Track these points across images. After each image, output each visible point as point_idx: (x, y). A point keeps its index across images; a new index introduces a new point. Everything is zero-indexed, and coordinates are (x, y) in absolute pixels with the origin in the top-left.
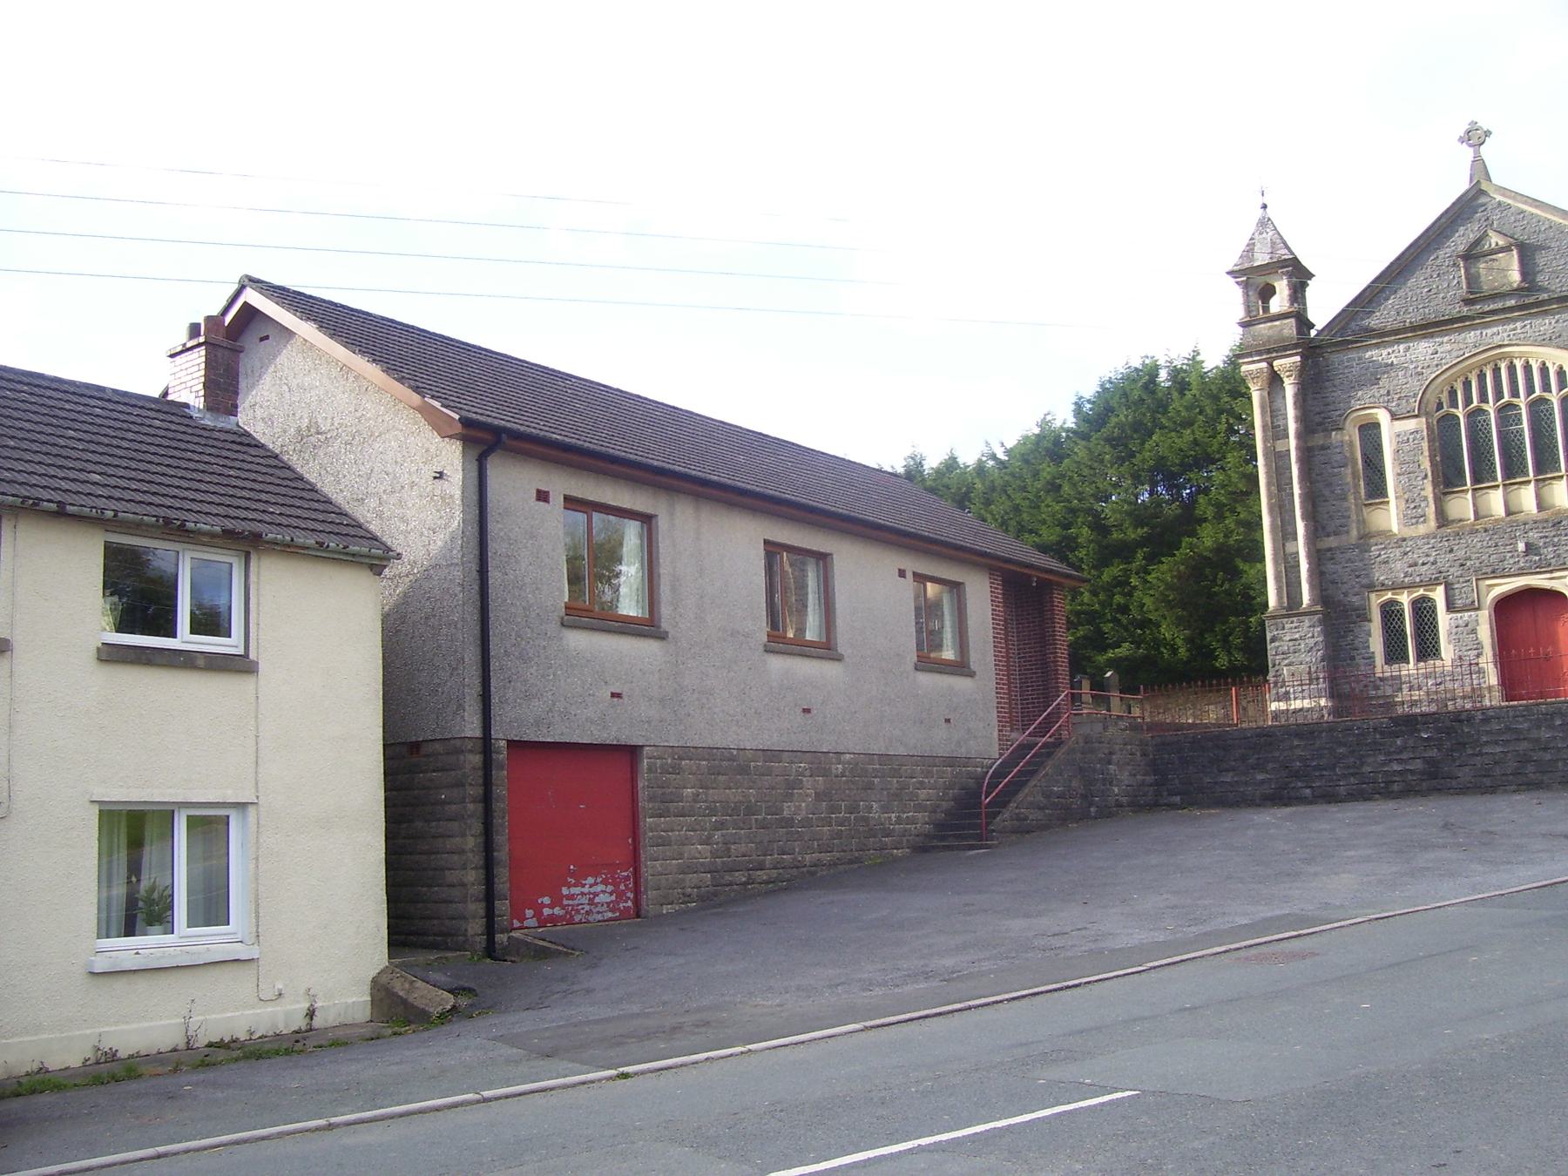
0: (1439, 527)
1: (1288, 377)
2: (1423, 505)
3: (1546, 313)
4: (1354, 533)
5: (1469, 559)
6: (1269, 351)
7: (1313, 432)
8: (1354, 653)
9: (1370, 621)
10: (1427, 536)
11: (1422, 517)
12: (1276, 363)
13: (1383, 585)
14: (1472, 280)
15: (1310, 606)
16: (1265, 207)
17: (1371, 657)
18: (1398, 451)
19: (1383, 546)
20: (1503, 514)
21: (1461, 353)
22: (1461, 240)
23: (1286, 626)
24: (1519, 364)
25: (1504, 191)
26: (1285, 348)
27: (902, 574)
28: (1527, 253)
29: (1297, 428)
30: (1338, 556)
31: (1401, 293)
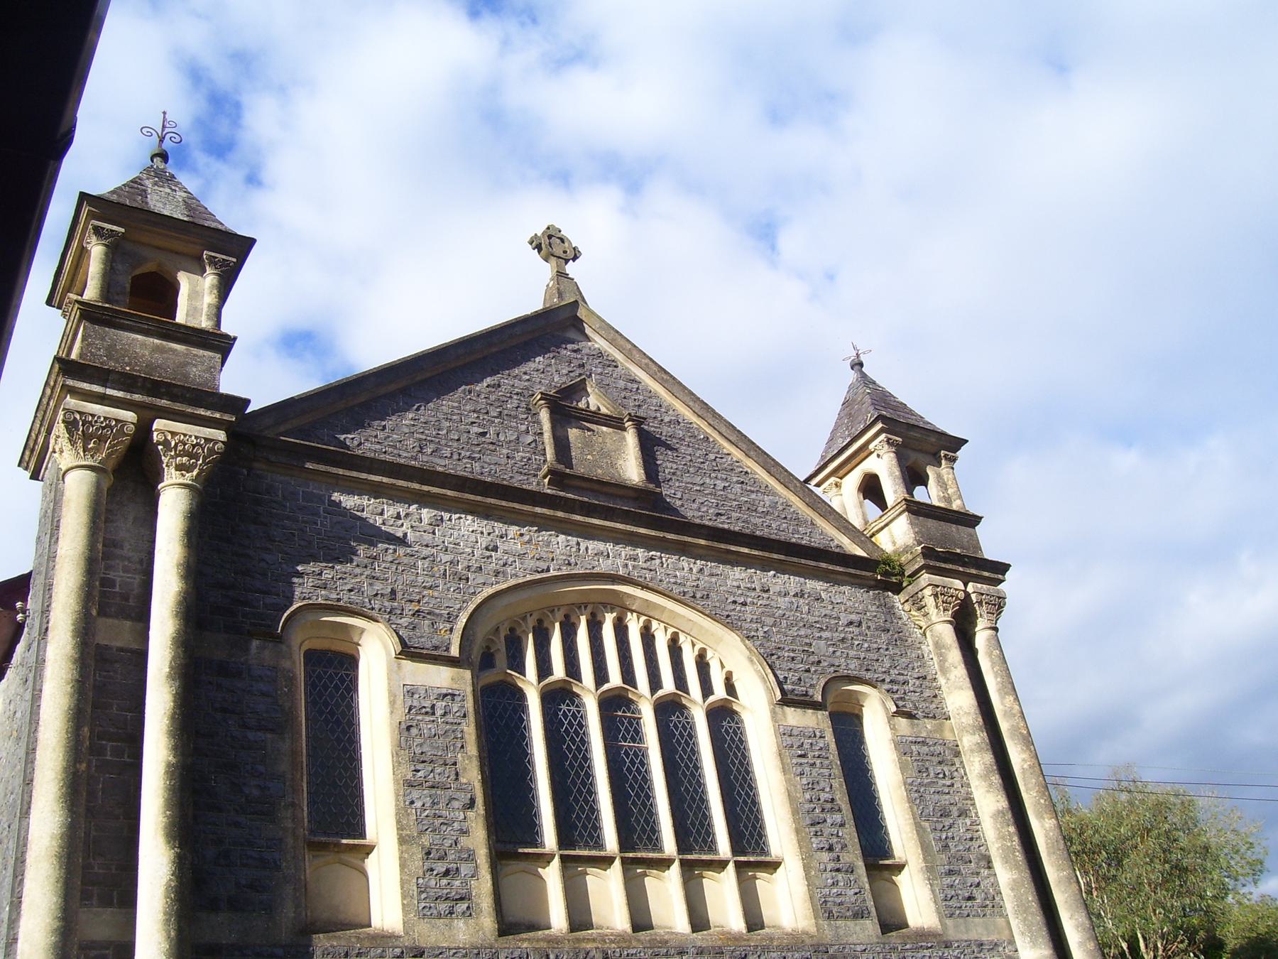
1: (180, 468)
2: (465, 869)
11: (462, 899)
12: (159, 424)
18: (409, 728)
21: (543, 565)
25: (615, 336)
28: (649, 445)
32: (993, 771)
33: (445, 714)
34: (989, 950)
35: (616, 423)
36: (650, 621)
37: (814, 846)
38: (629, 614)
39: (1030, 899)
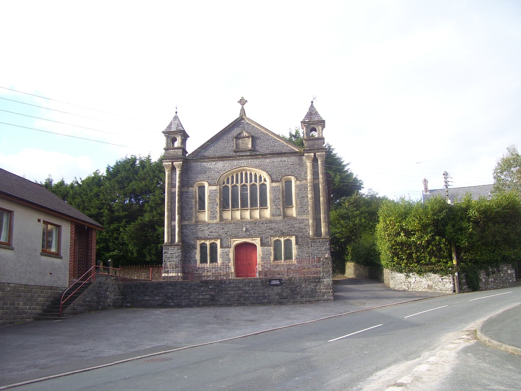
0: (220, 221)
1: (178, 168)
3: (258, 158)
4: (194, 220)
5: (228, 232)
6: (172, 159)
7: (184, 187)
8: (191, 259)
9: (196, 249)
10: (216, 224)
11: (215, 217)
13: (201, 238)
14: (237, 145)
15: (178, 243)
16: (176, 112)
17: (196, 261)
19: (202, 225)
20: (240, 219)
21: (232, 167)
22: (235, 132)
23: (170, 249)
24: (248, 173)
25: (249, 119)
26: (178, 159)
27: (39, 221)
28: (254, 139)
29: (179, 185)
30: (188, 227)
31: (216, 146)
33: (215, 193)
35: (248, 137)
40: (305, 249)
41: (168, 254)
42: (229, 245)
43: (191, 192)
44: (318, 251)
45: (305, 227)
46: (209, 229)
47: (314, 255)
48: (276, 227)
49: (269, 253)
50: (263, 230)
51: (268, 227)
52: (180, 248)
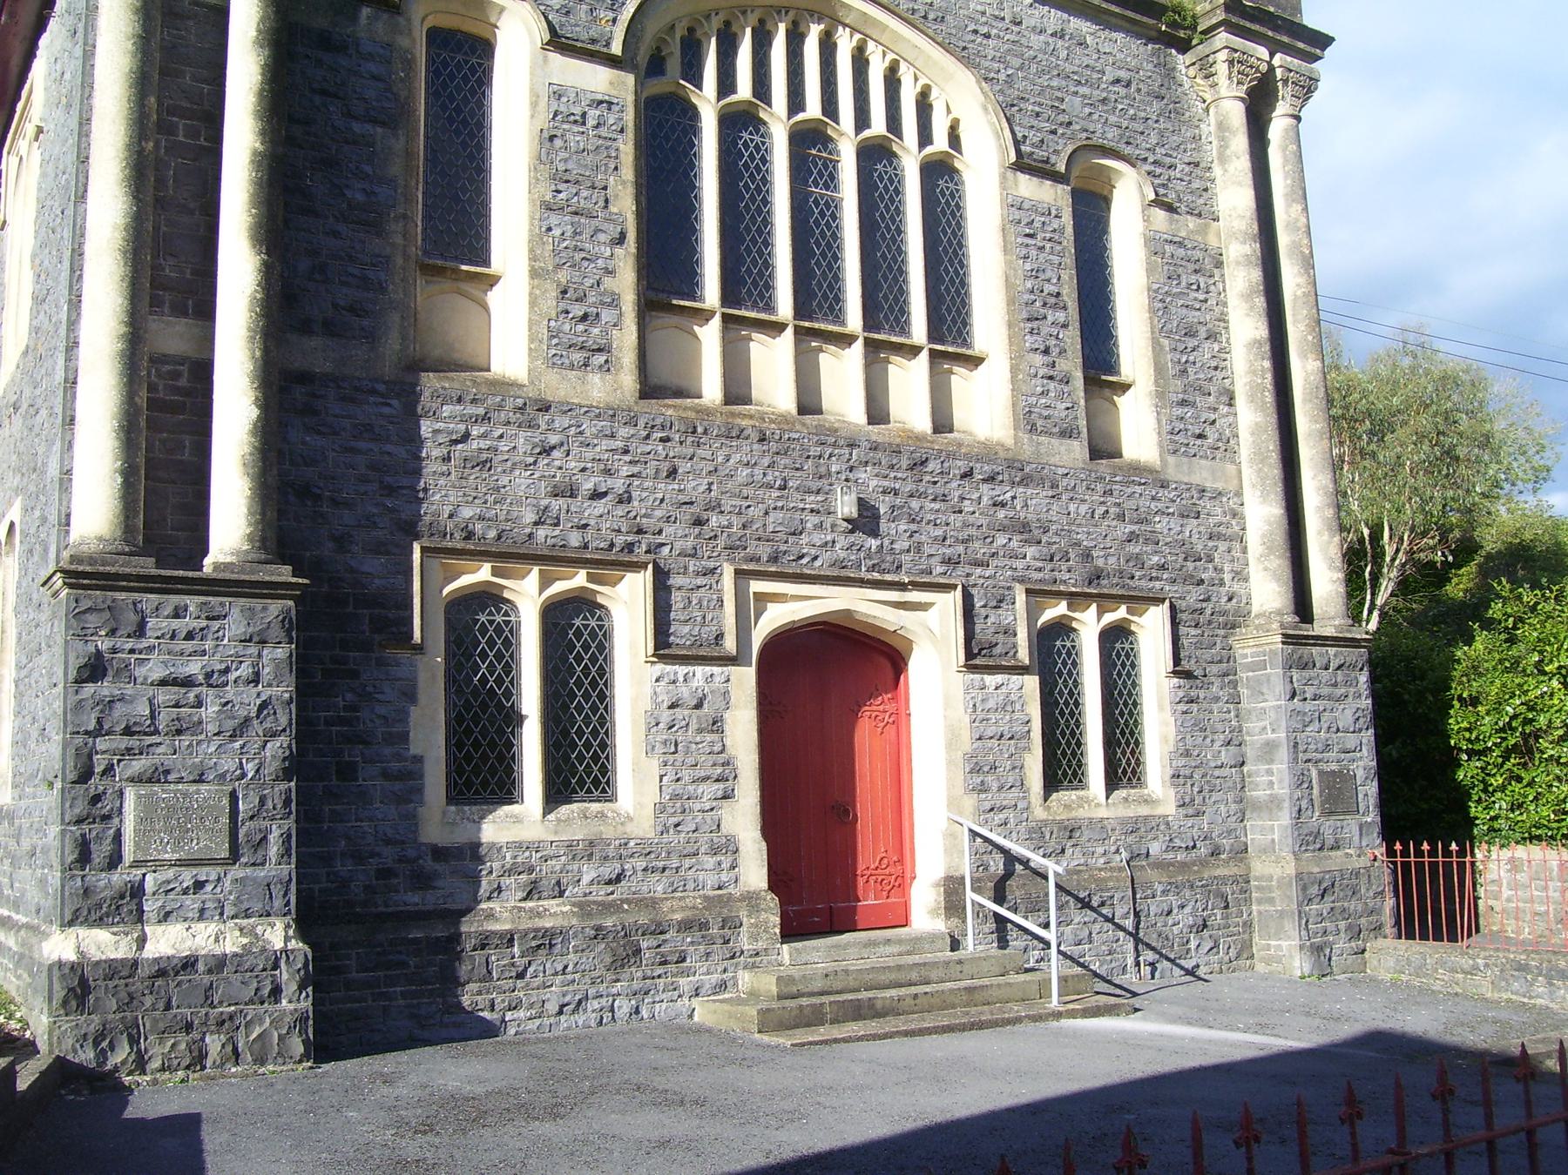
2: (607, 316)
5: (716, 507)
10: (611, 413)
11: (600, 350)
13: (469, 536)
15: (247, 562)
17: (409, 777)
18: (552, 138)
19: (481, 411)
23: (152, 622)
32: (1259, 291)
33: (598, 126)
34: (1211, 498)
36: (866, 41)
37: (1027, 345)
38: (840, 28)
39: (1271, 448)
40: (1215, 707)
41: (129, 690)
42: (720, 637)
43: (370, 57)
44: (1325, 726)
45: (1211, 544)
46: (543, 462)
47: (1308, 756)
48: (1053, 515)
49: (1017, 728)
50: (972, 531)
51: (1001, 514)
52: (285, 618)
